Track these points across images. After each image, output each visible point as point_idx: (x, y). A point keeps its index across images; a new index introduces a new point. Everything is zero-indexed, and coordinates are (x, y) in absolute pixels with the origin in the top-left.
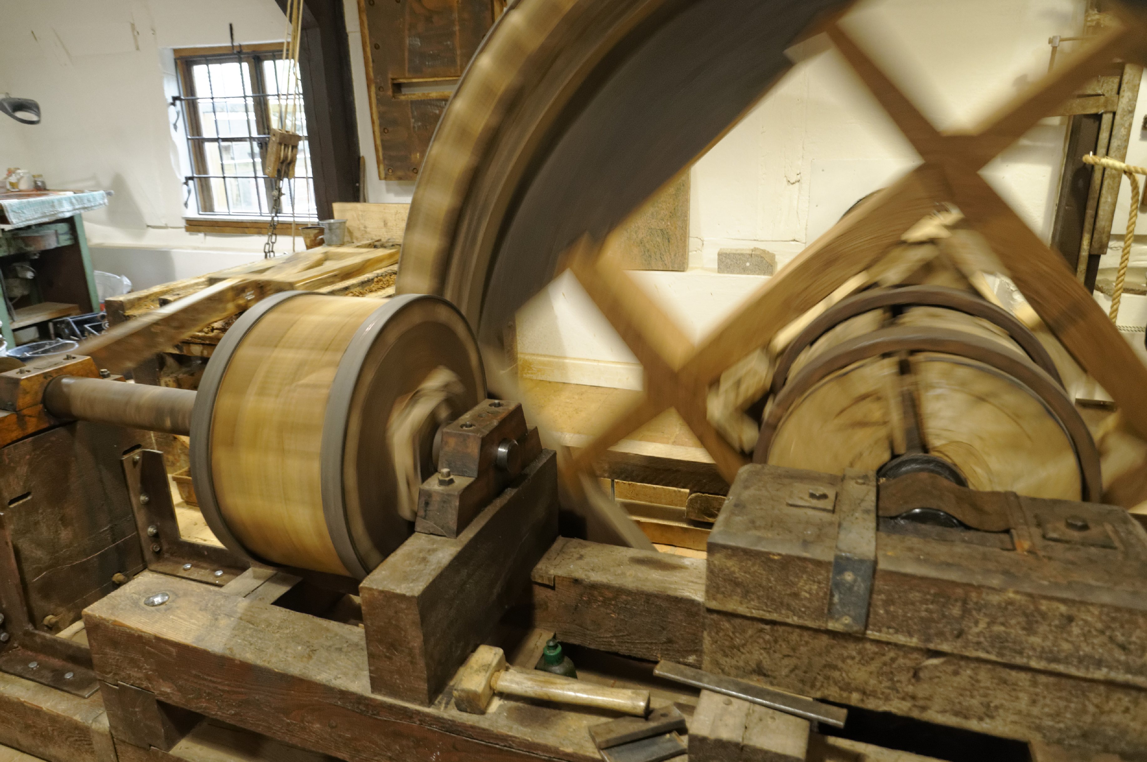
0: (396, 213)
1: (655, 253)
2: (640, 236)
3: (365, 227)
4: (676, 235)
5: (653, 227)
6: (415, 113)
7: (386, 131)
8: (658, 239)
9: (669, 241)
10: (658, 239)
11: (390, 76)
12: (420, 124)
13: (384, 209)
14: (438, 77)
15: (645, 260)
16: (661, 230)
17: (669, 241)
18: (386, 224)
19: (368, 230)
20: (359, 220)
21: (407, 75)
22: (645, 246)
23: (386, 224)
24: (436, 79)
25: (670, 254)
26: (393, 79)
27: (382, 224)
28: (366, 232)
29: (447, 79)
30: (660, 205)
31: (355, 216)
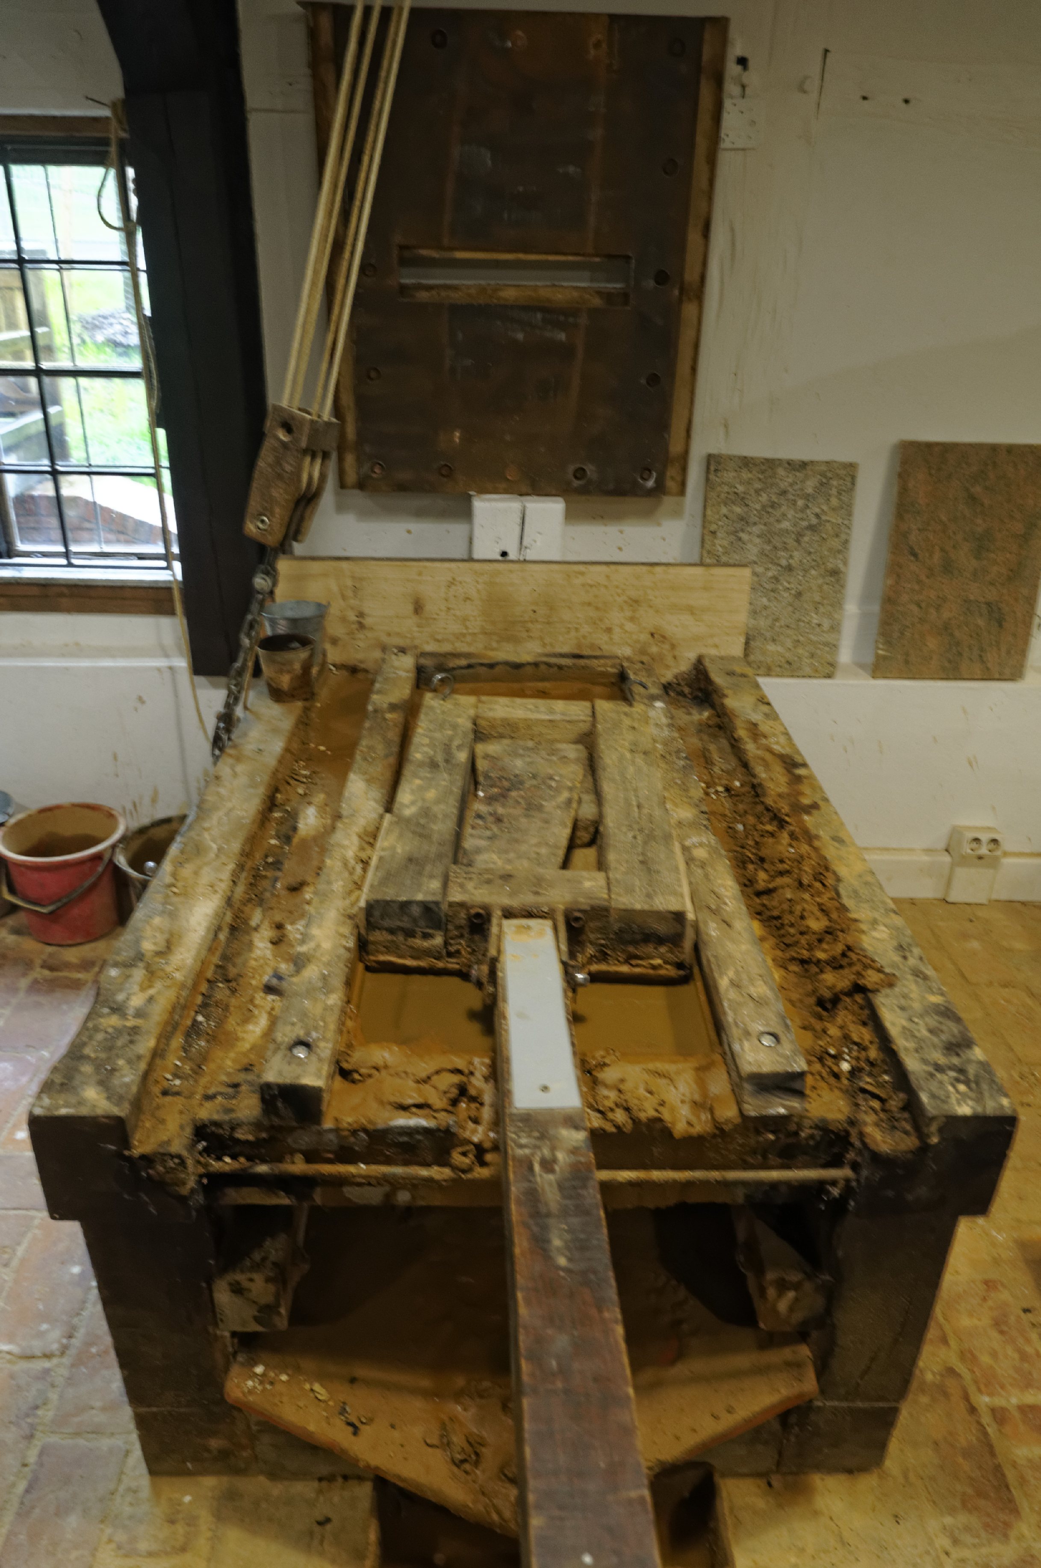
0: (451, 583)
1: (970, 647)
2: (946, 615)
3: (361, 615)
4: (1014, 612)
5: (972, 598)
6: (460, 336)
7: (373, 374)
8: (981, 622)
9: (1001, 626)
10: (981, 622)
11: (398, 239)
12: (469, 362)
13: (420, 574)
14: (525, 251)
15: (950, 661)
16: (988, 604)
17: (1001, 626)
18: (418, 608)
19: (368, 621)
20: (344, 597)
21: (446, 241)
22: (952, 635)
23: (418, 608)
24: (522, 256)
25: (999, 649)
26: (402, 248)
27: (410, 608)
28: (362, 626)
29: (551, 258)
30: (992, 555)
31: (335, 588)
